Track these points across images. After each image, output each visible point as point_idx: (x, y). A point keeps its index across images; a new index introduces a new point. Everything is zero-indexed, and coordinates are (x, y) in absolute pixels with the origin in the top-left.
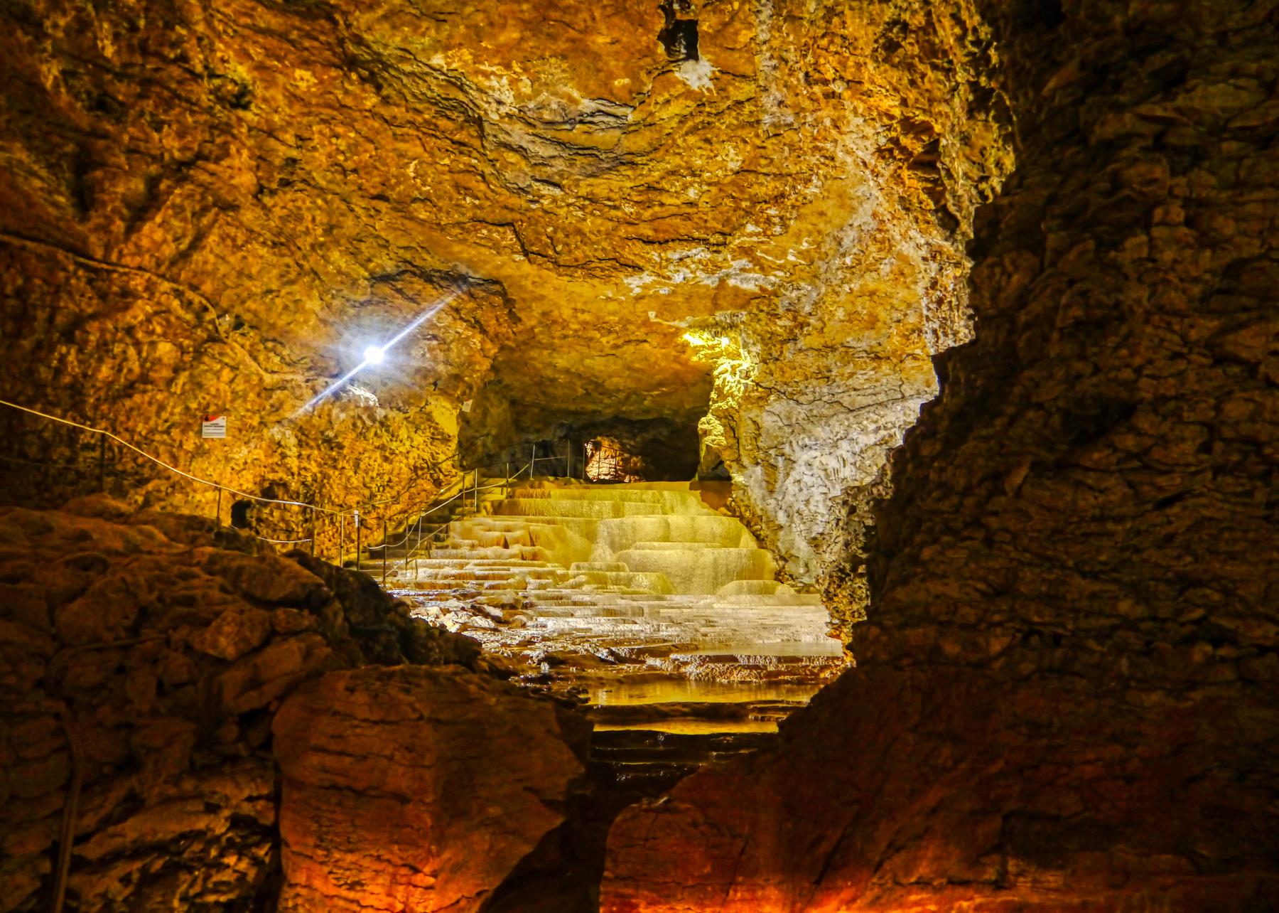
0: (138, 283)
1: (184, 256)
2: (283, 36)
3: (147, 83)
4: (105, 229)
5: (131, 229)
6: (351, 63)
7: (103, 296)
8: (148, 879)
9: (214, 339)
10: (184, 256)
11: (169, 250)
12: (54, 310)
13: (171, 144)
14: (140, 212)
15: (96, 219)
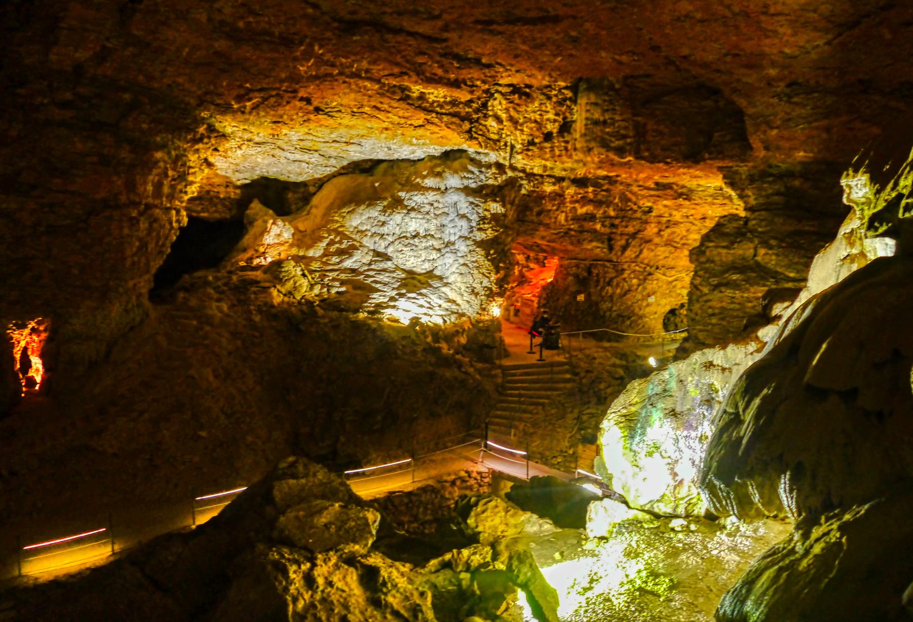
0: (625, 266)
1: (638, 256)
2: (659, 196)
3: (624, 217)
4: (616, 254)
5: (623, 253)
6: (680, 195)
7: (617, 271)
8: (590, 418)
9: (650, 274)
10: (638, 256)
11: (633, 256)
12: (605, 278)
13: (631, 230)
14: (624, 248)
15: (614, 252)
